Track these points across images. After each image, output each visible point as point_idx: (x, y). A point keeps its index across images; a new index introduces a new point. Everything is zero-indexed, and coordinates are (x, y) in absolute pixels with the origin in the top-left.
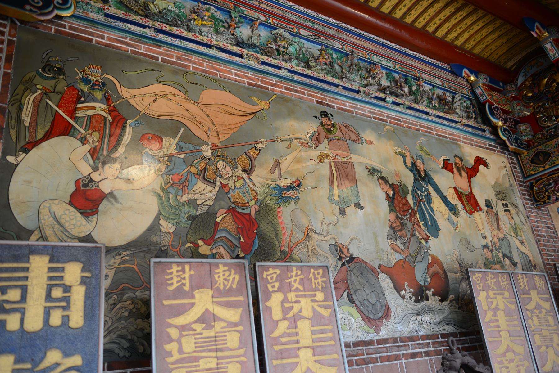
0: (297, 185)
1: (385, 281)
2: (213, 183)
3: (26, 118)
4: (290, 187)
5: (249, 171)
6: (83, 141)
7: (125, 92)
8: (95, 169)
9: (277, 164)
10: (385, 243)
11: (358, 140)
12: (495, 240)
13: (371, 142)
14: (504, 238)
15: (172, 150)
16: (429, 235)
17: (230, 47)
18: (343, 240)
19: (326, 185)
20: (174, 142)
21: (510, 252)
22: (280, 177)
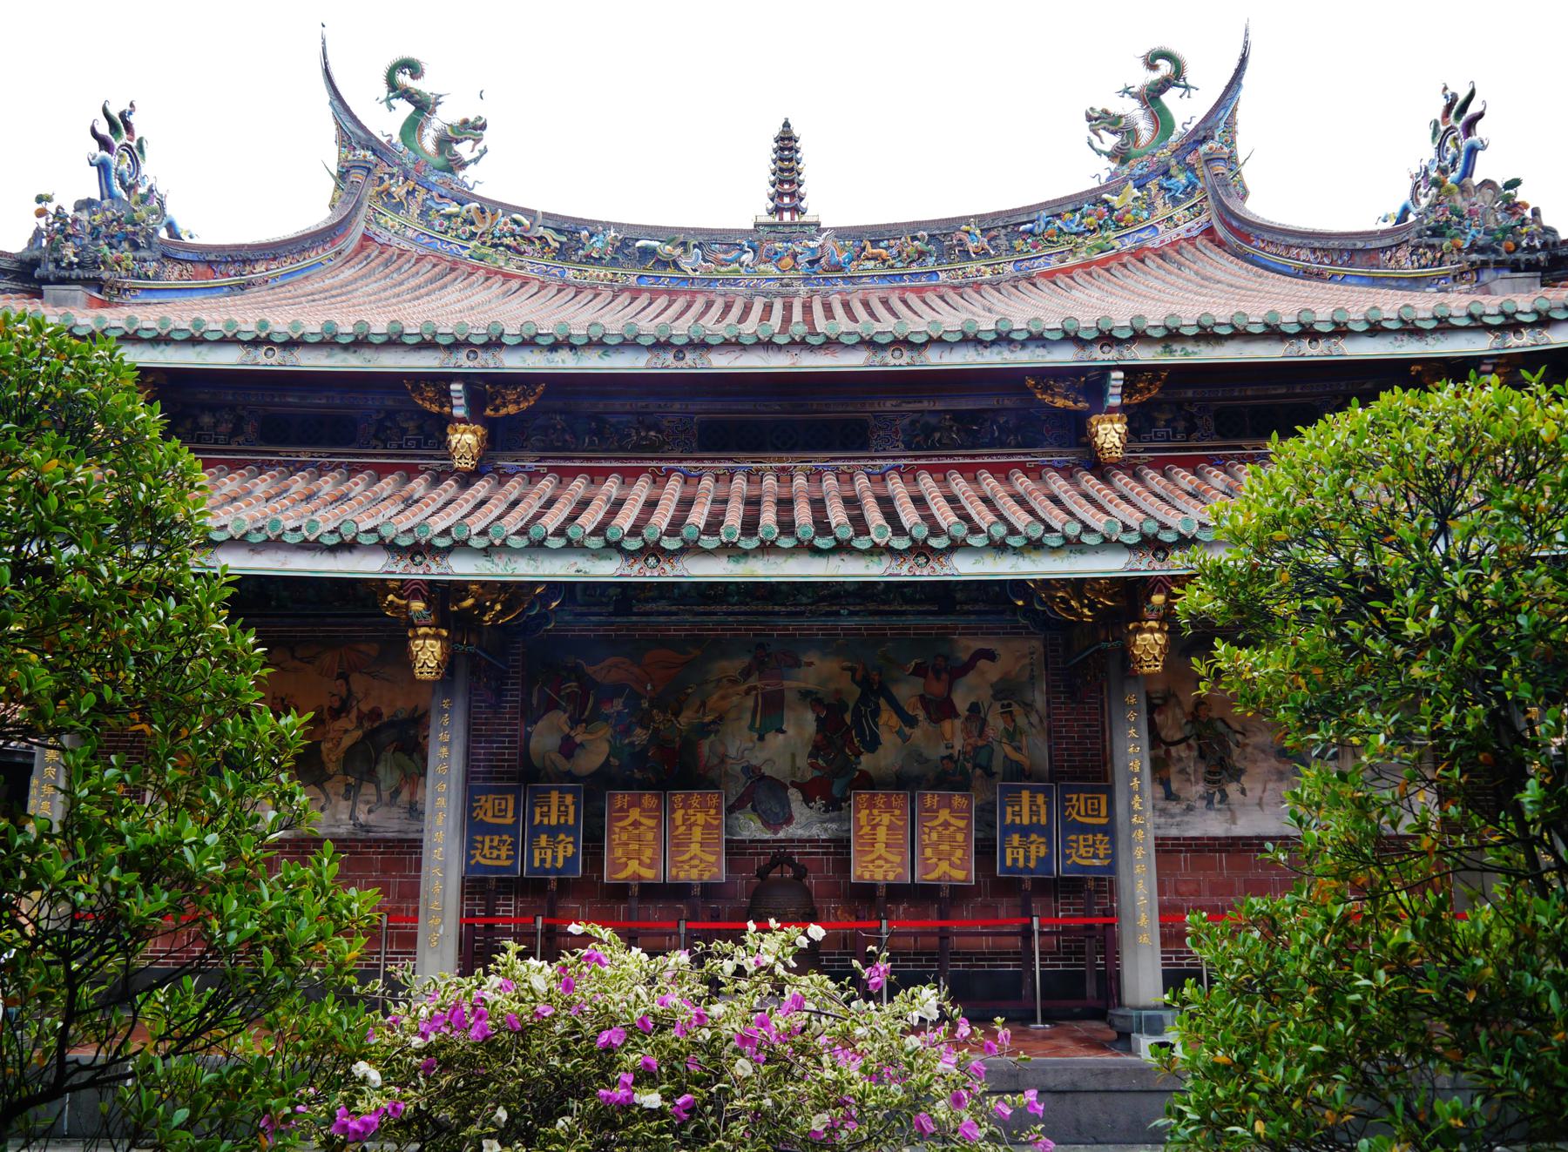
0: (720, 719)
1: (794, 795)
2: (648, 729)
3: (535, 702)
4: (713, 722)
5: (677, 714)
6: (565, 712)
7: (590, 670)
8: (572, 729)
9: (703, 704)
10: (803, 762)
11: (797, 664)
12: (969, 748)
13: (810, 664)
15: (620, 708)
17: (668, 608)
18: (754, 762)
19: (748, 716)
20: (621, 700)
22: (704, 714)
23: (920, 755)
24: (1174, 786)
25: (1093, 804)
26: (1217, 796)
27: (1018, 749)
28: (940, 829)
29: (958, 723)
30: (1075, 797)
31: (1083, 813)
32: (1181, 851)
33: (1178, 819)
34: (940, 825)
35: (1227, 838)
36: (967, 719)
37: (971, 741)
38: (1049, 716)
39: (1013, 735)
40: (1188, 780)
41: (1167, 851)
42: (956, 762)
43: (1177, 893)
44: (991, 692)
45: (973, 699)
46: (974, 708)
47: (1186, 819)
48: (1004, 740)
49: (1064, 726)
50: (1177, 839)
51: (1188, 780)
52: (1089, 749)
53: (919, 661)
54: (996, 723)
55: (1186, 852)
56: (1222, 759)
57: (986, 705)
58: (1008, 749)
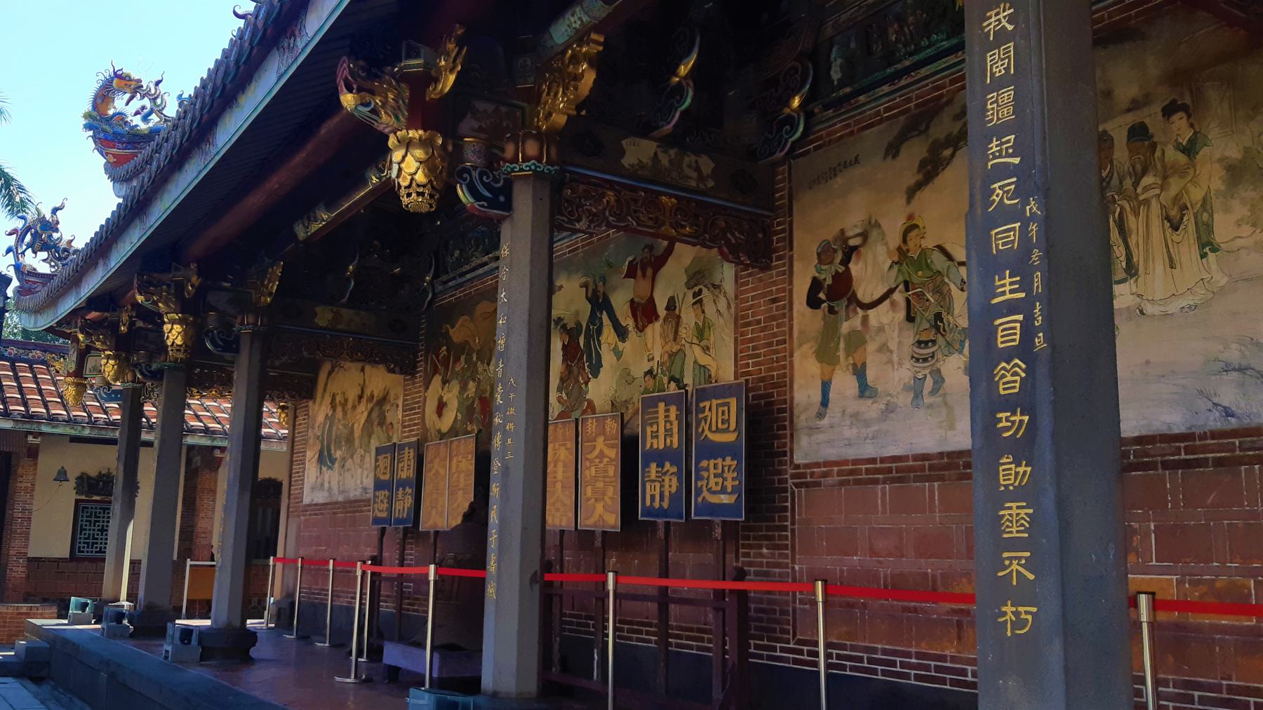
12: (666, 357)
14: (680, 350)
16: (590, 376)
21: (682, 372)
23: (629, 374)
24: (871, 375)
25: (723, 412)
26: (929, 383)
27: (706, 349)
28: (597, 461)
29: (657, 325)
30: (707, 404)
31: (714, 428)
32: (876, 482)
33: (875, 428)
34: (596, 457)
35: (941, 455)
36: (665, 320)
37: (667, 348)
38: (736, 297)
39: (701, 332)
40: (890, 362)
41: (858, 482)
42: (654, 377)
43: (873, 553)
44: (685, 280)
45: (670, 294)
46: (671, 306)
47: (884, 426)
48: (695, 341)
49: (751, 307)
50: (873, 461)
51: (890, 362)
52: (775, 335)
53: (630, 259)
54: (689, 317)
55: (884, 483)
56: (938, 317)
57: (681, 297)
58: (697, 350)
